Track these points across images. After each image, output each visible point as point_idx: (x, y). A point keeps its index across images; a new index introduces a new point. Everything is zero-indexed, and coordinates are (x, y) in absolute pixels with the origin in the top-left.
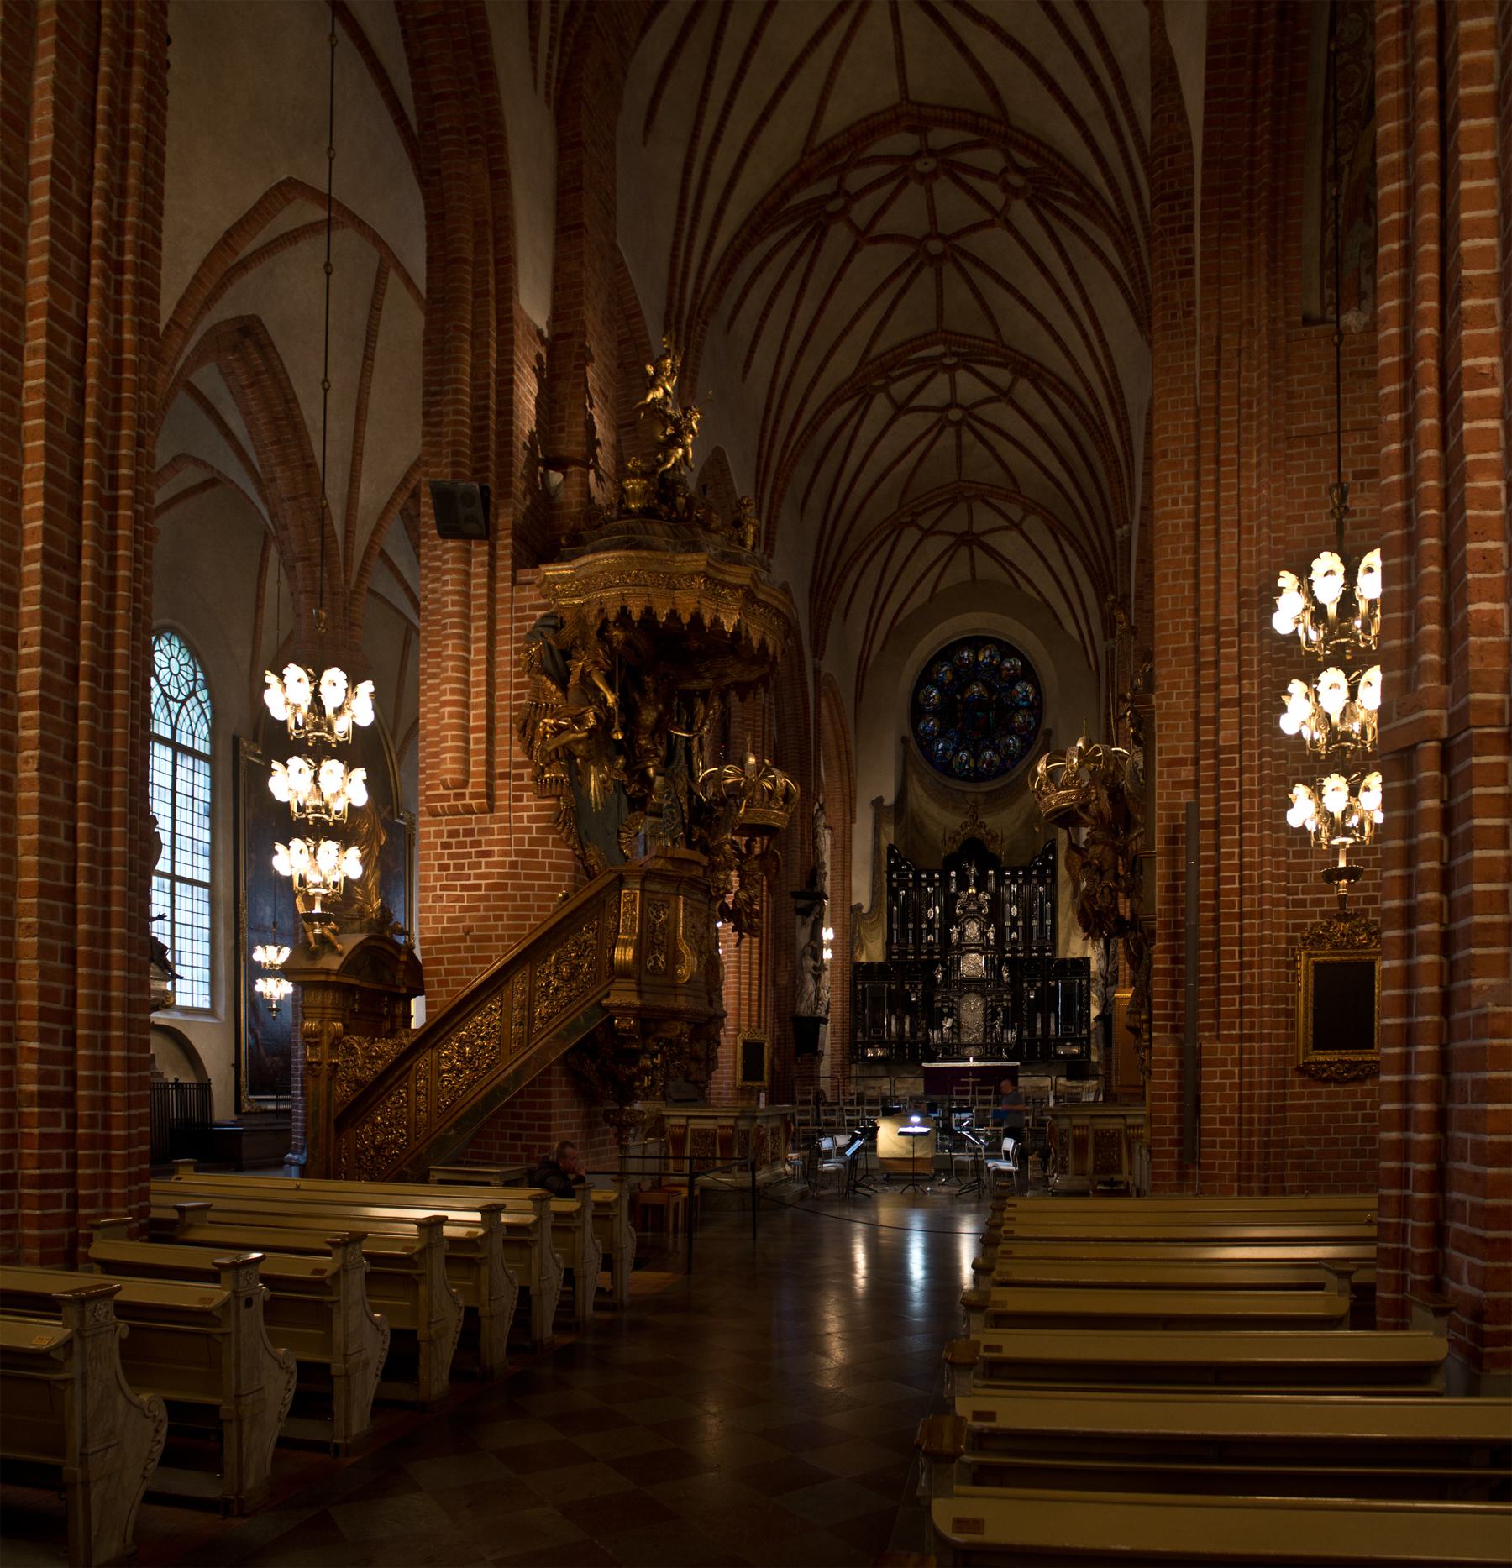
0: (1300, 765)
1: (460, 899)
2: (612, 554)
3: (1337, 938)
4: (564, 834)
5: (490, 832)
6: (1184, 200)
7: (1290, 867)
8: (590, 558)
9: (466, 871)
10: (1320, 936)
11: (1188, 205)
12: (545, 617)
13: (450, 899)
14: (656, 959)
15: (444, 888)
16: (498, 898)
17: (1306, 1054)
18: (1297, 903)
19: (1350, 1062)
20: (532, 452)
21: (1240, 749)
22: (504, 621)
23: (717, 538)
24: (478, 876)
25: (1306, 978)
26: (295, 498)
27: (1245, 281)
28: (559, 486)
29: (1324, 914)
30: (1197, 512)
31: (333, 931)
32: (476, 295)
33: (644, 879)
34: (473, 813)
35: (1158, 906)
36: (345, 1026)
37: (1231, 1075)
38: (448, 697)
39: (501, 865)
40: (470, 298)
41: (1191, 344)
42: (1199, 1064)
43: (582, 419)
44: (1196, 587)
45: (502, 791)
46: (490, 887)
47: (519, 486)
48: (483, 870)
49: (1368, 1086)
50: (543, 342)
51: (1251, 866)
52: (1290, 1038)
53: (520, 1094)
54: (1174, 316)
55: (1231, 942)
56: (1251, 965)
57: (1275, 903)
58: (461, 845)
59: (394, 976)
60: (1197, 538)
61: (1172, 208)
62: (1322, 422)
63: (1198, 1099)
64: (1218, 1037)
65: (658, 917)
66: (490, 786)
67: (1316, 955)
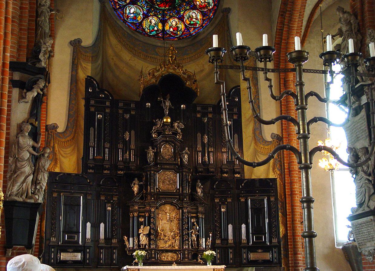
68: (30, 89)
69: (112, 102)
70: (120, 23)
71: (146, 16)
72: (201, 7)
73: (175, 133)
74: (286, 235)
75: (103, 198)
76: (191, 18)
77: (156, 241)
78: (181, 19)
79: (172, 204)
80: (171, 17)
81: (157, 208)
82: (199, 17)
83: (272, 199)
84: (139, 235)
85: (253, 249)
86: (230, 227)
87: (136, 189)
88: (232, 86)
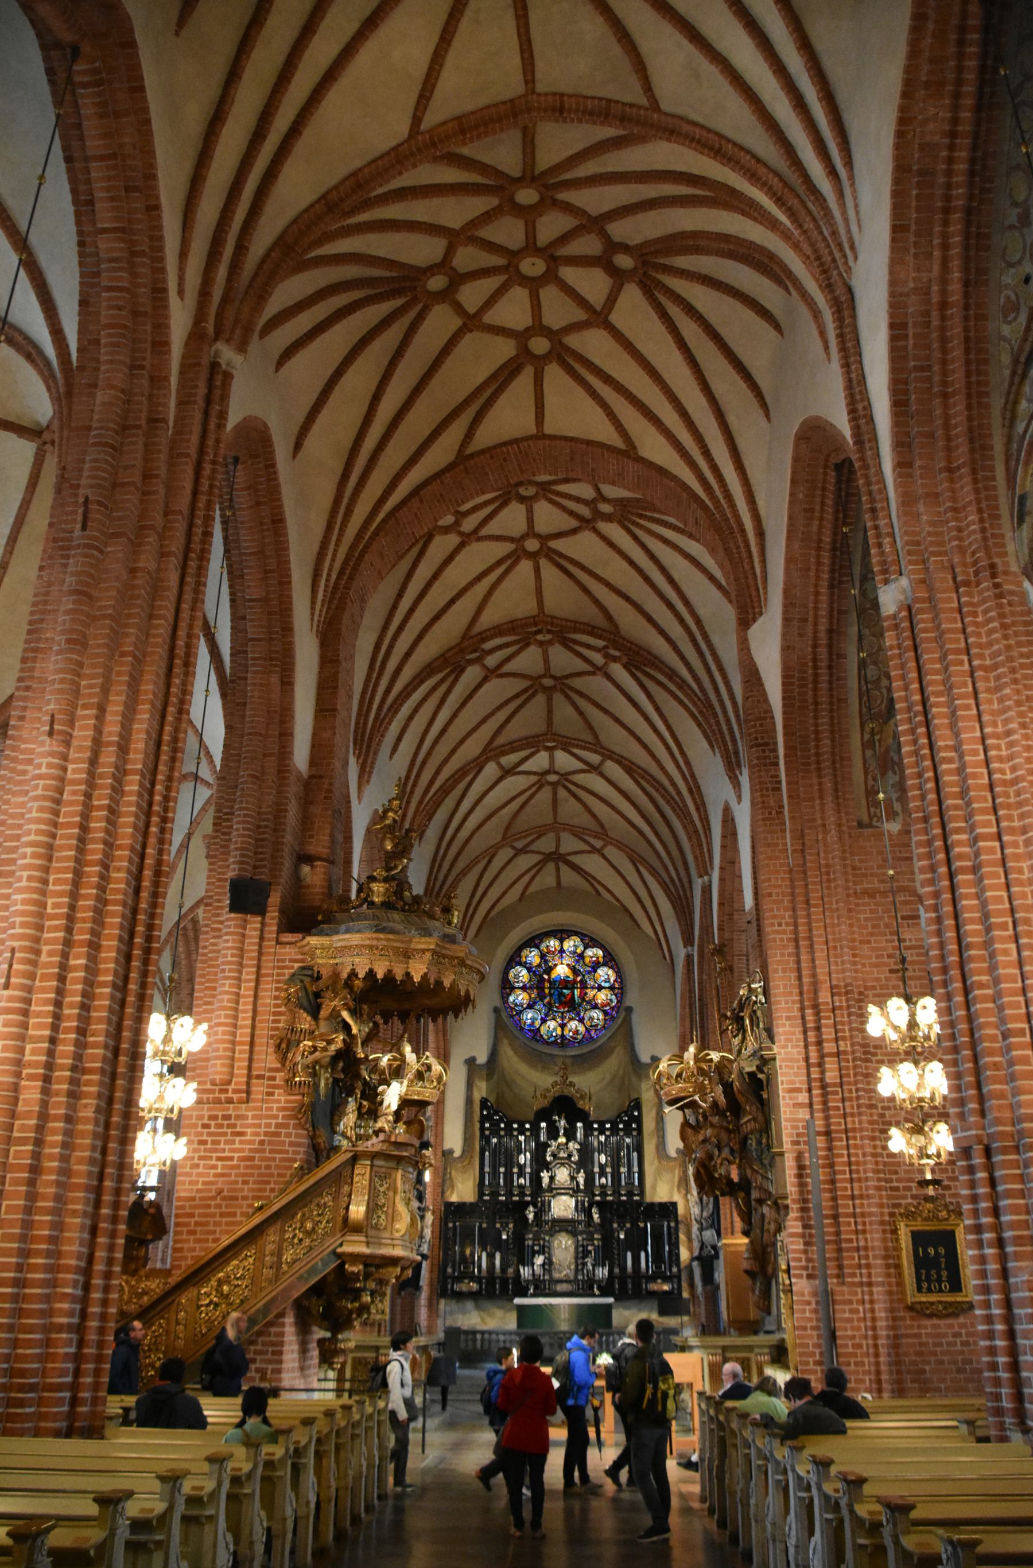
1: (214, 1167)
3: (925, 1214)
5: (246, 1117)
7: (885, 1164)
9: (222, 1146)
11: (775, 750)
12: (303, 968)
13: (205, 1167)
15: (200, 1158)
16: (247, 1167)
18: (892, 1189)
21: (841, 1085)
22: (267, 968)
29: (914, 1197)
30: (796, 932)
39: (252, 1142)
41: (784, 831)
44: (800, 978)
45: (259, 1089)
48: (237, 1146)
49: (962, 1320)
51: (858, 1163)
55: (847, 1215)
56: (864, 1232)
58: (221, 1126)
60: (797, 947)
61: (764, 751)
64: (843, 1283)
66: (248, 1084)
70: (517, 1033)
71: (544, 1021)
73: (570, 1156)
75: (498, 1226)
76: (591, 1018)
77: (550, 1271)
78: (581, 1021)
79: (567, 1231)
80: (571, 1019)
81: (551, 1236)
82: (601, 1017)
83: (672, 1224)
84: (533, 1264)
85: (653, 1278)
86: (629, 1255)
87: (531, 1216)
88: (635, 1096)
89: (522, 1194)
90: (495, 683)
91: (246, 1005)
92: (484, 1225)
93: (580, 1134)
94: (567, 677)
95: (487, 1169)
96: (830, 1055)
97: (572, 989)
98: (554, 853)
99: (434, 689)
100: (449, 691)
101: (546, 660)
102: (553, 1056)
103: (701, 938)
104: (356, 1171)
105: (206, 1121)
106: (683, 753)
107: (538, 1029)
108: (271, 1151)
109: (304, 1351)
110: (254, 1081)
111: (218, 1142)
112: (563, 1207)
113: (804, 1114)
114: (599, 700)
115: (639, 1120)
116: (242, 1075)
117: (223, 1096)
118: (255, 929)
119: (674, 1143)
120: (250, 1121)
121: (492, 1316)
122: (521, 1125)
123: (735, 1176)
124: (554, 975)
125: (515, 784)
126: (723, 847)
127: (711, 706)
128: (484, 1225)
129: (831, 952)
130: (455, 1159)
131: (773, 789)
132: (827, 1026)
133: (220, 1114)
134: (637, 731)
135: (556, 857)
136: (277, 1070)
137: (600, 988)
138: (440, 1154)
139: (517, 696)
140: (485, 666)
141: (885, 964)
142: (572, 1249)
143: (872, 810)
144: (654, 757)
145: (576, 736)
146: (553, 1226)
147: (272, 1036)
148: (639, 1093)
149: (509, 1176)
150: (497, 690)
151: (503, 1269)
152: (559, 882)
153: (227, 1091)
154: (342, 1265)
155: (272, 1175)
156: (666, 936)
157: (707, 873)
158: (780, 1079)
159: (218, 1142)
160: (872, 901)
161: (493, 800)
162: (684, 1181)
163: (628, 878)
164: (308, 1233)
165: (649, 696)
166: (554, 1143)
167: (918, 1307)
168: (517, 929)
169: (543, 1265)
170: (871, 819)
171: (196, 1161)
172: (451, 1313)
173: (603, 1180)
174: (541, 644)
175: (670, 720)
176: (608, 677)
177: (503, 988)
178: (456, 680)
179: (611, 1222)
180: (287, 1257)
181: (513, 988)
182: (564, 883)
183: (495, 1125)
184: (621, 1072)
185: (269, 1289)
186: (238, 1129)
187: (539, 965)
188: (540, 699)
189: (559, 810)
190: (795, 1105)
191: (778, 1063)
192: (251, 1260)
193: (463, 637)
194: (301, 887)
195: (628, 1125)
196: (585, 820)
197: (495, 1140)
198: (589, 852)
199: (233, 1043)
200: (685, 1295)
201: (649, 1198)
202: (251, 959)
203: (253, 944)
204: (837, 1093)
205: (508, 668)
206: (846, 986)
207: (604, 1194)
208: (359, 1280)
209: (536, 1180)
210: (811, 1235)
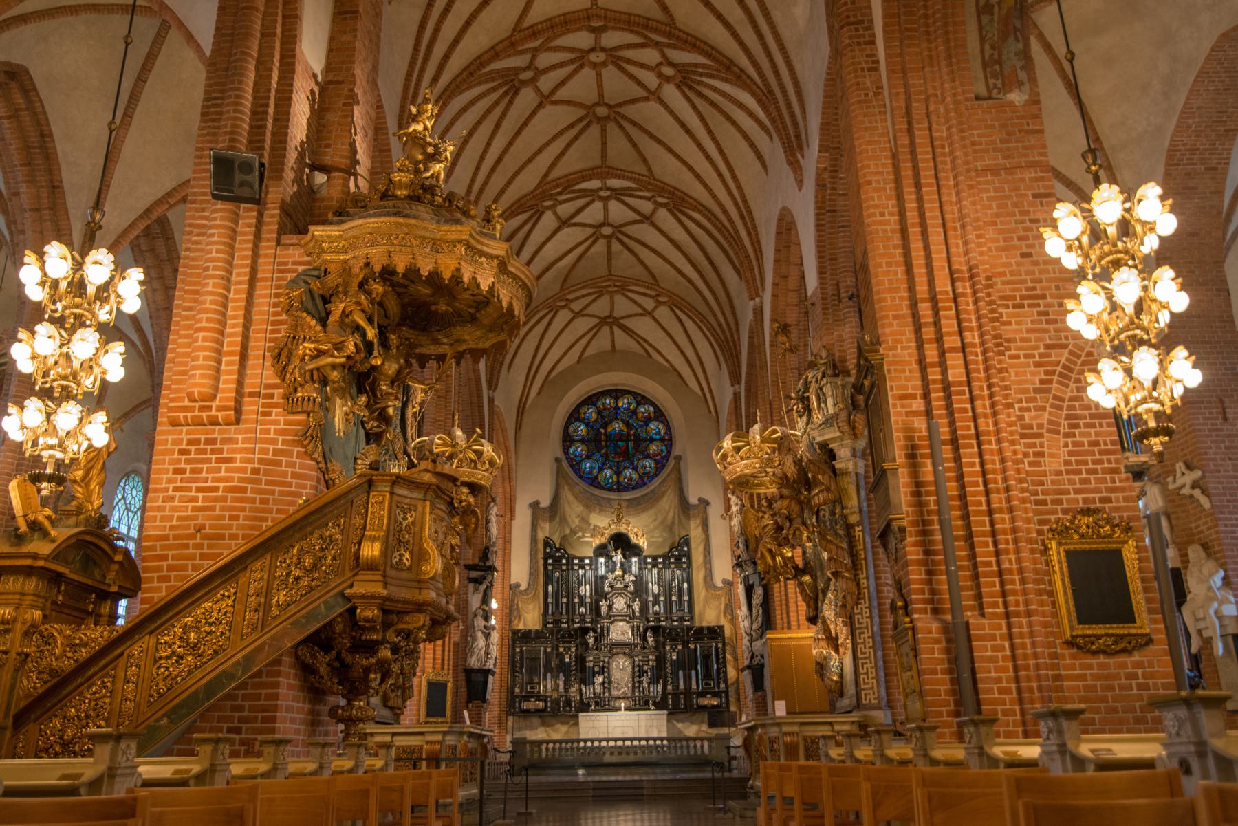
0: (1023, 397)
2: (383, 219)
3: (1084, 529)
4: (310, 448)
6: (866, 25)
8: (360, 221)
9: (204, 475)
10: (1066, 527)
11: (870, 28)
14: (401, 556)
15: (176, 489)
16: (235, 500)
17: (1072, 628)
18: (1037, 503)
19: (1117, 635)
20: (301, 156)
22: (264, 271)
23: (473, 223)
24: (215, 480)
25: (1060, 562)
26: (37, 210)
27: (927, 69)
28: (321, 185)
29: (1065, 511)
31: (48, 518)
32: (263, 35)
33: (394, 483)
34: (219, 424)
35: (905, 508)
36: (45, 617)
37: (1002, 649)
38: (204, 324)
39: (244, 470)
40: (259, 35)
42: (969, 639)
43: (348, 140)
45: (251, 407)
46: (226, 490)
47: (289, 175)
48: (223, 474)
49: (1136, 657)
50: (317, 83)
52: (1055, 615)
53: (243, 685)
54: (867, 95)
56: (1007, 552)
57: (1024, 501)
58: (204, 452)
59: (104, 576)
61: (857, 30)
62: (1001, 161)
63: (973, 672)
64: (983, 615)
65: (405, 518)
67: (1066, 544)
68: (481, 583)
69: (568, 560)
70: (577, 479)
71: (601, 469)
72: (655, 455)
73: (626, 586)
74: (737, 681)
75: (561, 650)
76: (645, 467)
78: (635, 469)
80: (626, 468)
83: (720, 645)
85: (702, 695)
86: (681, 673)
87: (591, 641)
88: (683, 533)
89: (583, 621)
90: (549, 109)
91: (235, 312)
92: (549, 650)
93: (635, 569)
94: (620, 105)
95: (550, 600)
96: (953, 350)
97: (627, 441)
98: (609, 317)
99: (489, 111)
100: (504, 114)
101: (600, 86)
102: (610, 500)
103: (747, 373)
104: (372, 500)
105: (184, 446)
106: (734, 177)
107: (596, 477)
108: (268, 483)
109: (314, 723)
110: (246, 399)
111: (200, 471)
112: (620, 632)
113: (920, 424)
114: (652, 130)
115: (688, 555)
116: (229, 391)
117: (204, 415)
118: (249, 226)
119: (723, 569)
120: (240, 445)
121: (556, 731)
122: (582, 560)
123: (799, 562)
124: (609, 430)
125: (570, 236)
126: (776, 261)
127: (771, 92)
128: (549, 650)
129: (950, 233)
130: (521, 592)
131: (870, 70)
132: (947, 318)
133: (202, 437)
134: (691, 162)
135: (610, 321)
136: (275, 386)
137: (652, 440)
138: (507, 589)
139: (572, 126)
140: (538, 90)
141: (1015, 248)
142: (629, 669)
143: (991, 82)
144: (706, 186)
145: (630, 169)
146: (611, 649)
147: (269, 349)
148: (688, 530)
149: (570, 605)
150: (553, 118)
151: (566, 690)
152: (613, 346)
153: (210, 408)
154: (352, 610)
155: (270, 511)
156: (711, 391)
157: (758, 295)
158: (888, 384)
159: (200, 471)
160: (996, 178)
161: (550, 252)
162: (730, 609)
163: (677, 339)
164: (308, 571)
165: (702, 119)
166: (610, 576)
167: (1080, 641)
168: (575, 388)
169: (603, 684)
170: (989, 91)
171: (170, 493)
172: (520, 729)
173: (657, 608)
174: (594, 65)
175: (722, 145)
176: (661, 101)
177: (564, 441)
178: (511, 103)
179: (664, 645)
180: (281, 597)
181: (572, 441)
182: (617, 348)
183: (557, 561)
184: (671, 515)
185: (254, 637)
186: (225, 455)
187: (596, 421)
188: (595, 130)
189: (614, 262)
190: (908, 414)
191: (886, 368)
192: (230, 602)
193: (514, 30)
194: (314, 200)
195: (678, 559)
196: (638, 271)
197: (557, 574)
198: (641, 315)
199: (219, 352)
200: (733, 708)
201: (697, 624)
202: (244, 258)
203: (246, 241)
204: (963, 393)
205: (562, 94)
206: (970, 269)
207: (657, 620)
208: (373, 629)
209: (597, 609)
210: (934, 563)
